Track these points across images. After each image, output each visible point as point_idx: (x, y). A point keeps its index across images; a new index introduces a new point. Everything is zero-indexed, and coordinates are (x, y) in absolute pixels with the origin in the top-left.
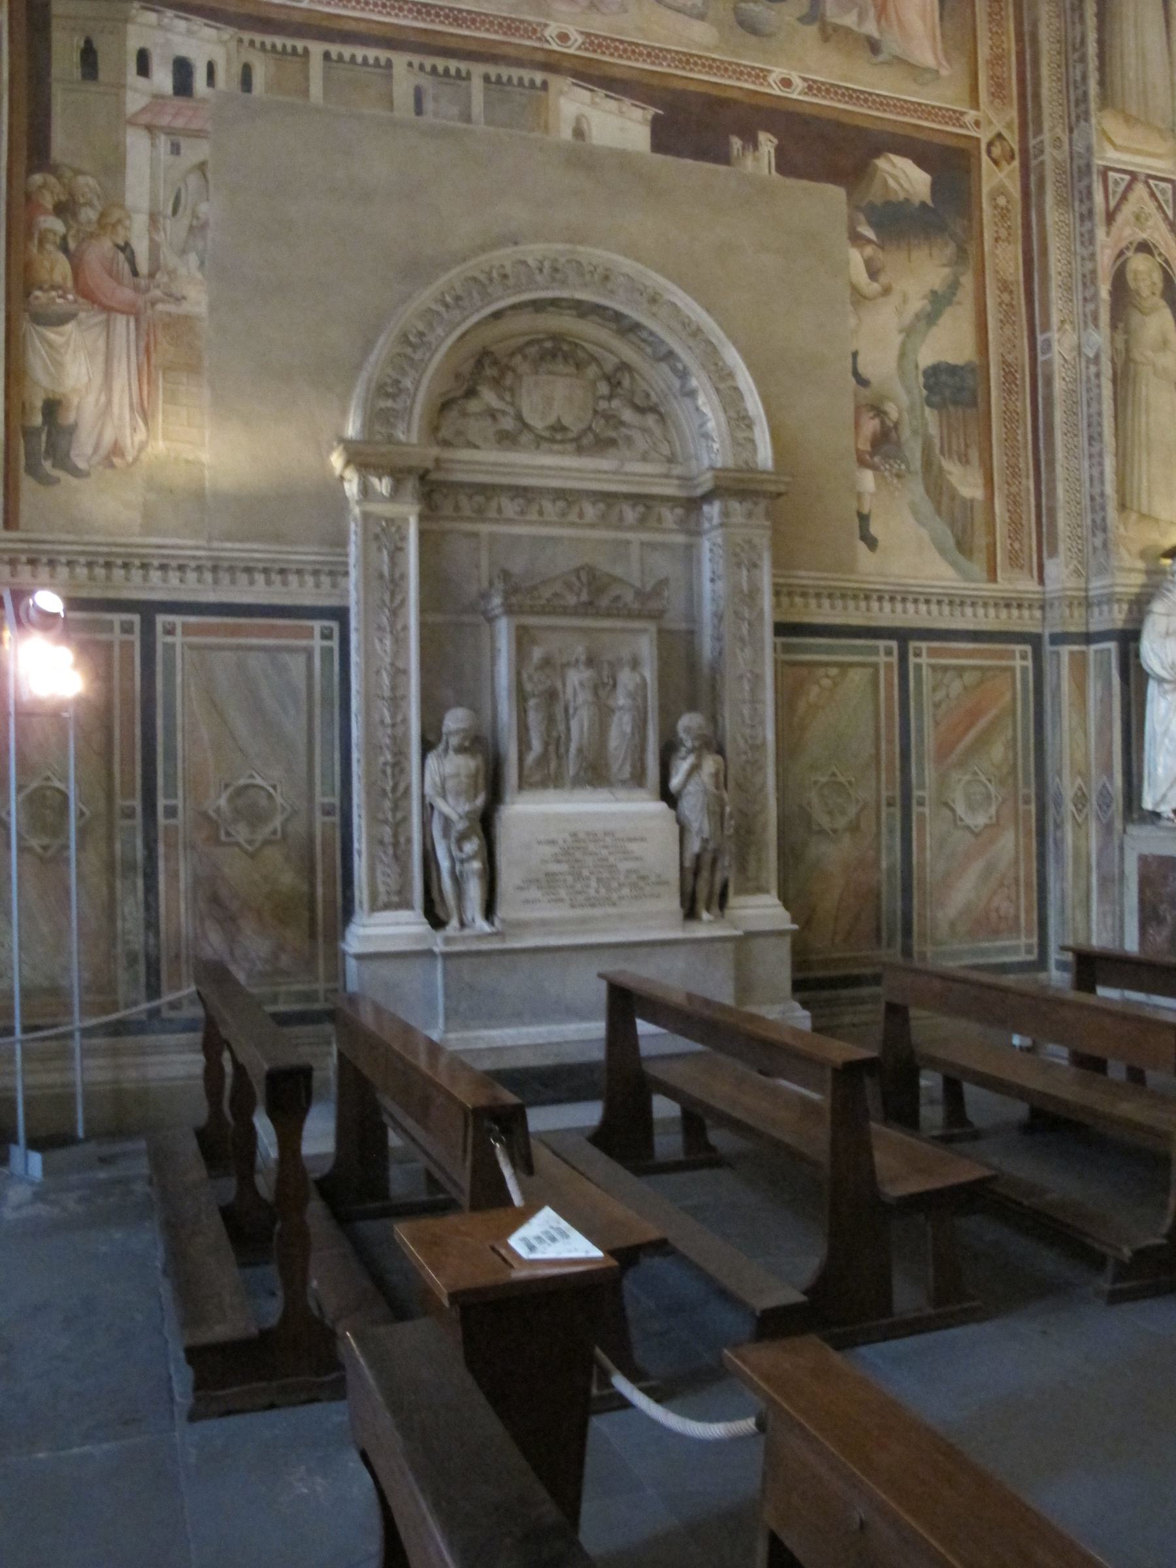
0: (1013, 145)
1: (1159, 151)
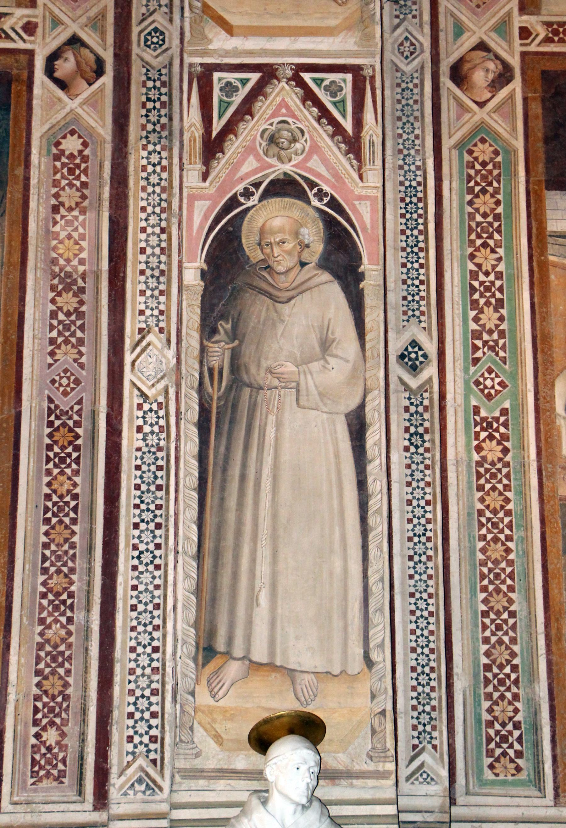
0: (100, 51)
1: (332, 22)
